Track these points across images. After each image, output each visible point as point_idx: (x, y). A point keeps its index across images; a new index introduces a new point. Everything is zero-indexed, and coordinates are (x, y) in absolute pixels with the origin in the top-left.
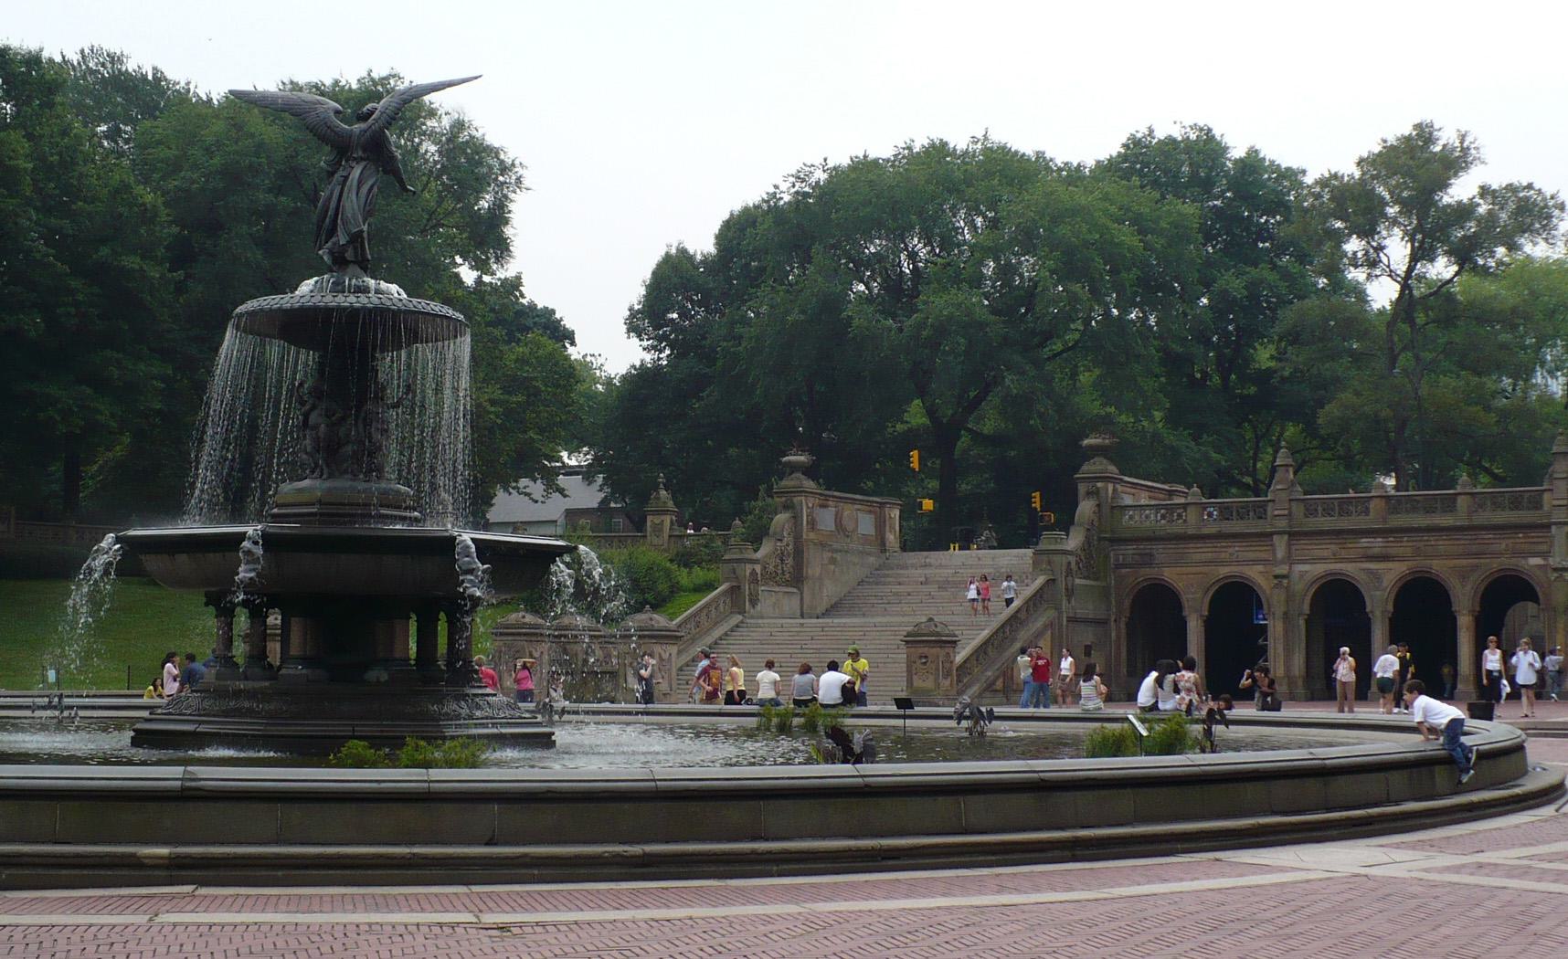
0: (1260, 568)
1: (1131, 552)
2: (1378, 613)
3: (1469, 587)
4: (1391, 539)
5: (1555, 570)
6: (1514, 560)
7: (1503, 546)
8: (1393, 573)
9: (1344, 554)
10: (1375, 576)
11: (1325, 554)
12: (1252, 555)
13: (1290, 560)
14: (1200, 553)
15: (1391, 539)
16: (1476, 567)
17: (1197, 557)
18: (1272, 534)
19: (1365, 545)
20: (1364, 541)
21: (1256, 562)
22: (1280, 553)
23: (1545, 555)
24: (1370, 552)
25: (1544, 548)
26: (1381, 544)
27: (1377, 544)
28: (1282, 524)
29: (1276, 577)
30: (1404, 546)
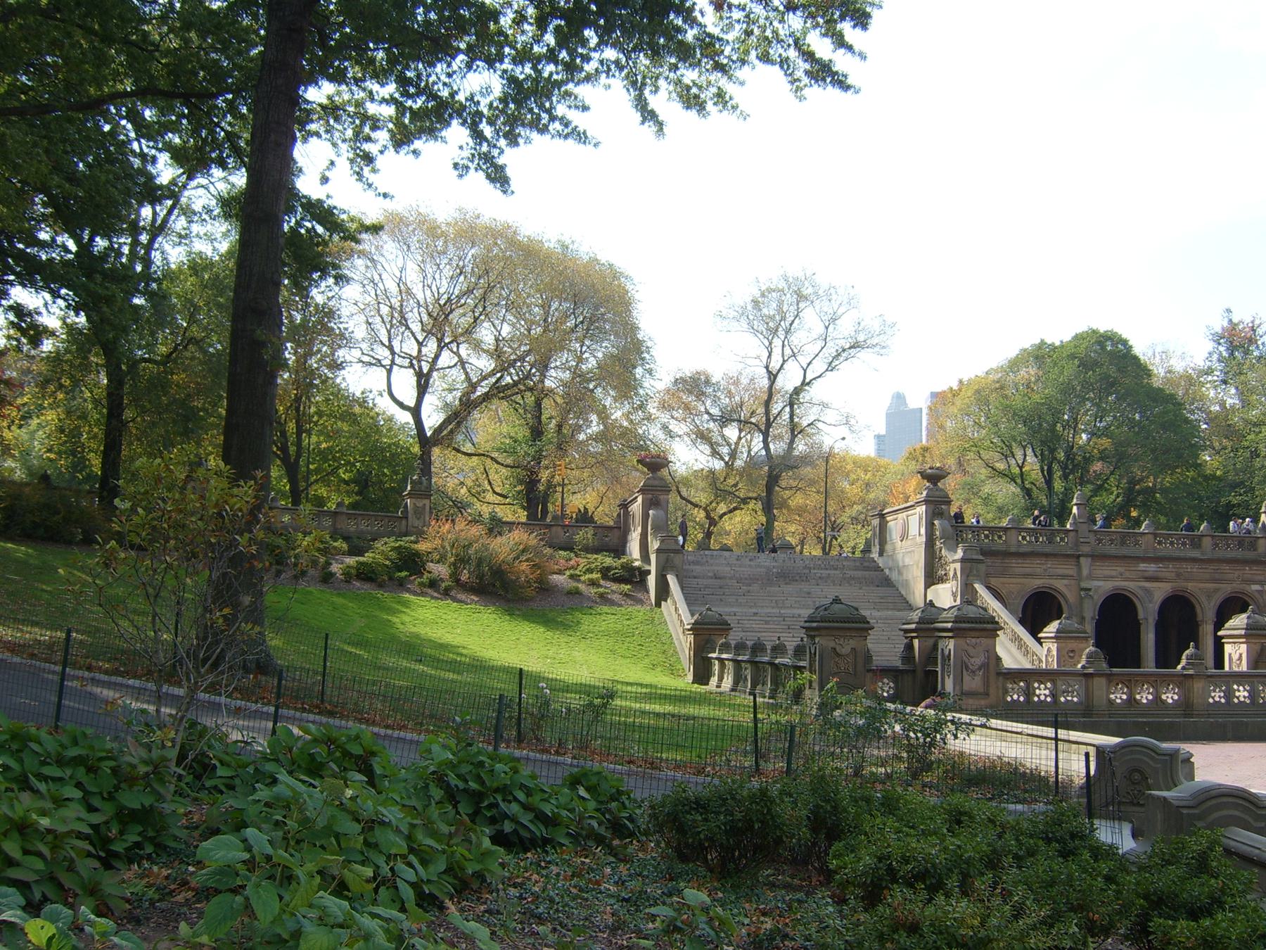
0: (1065, 582)
3: (1212, 604)
6: (1241, 586)
8: (1160, 591)
9: (1127, 574)
10: (1146, 590)
11: (1114, 573)
12: (1060, 572)
13: (1091, 577)
14: (1017, 566)
16: (1216, 590)
17: (1018, 571)
18: (1079, 557)
20: (1142, 566)
21: (1064, 577)
22: (1085, 572)
24: (1146, 574)
27: (1151, 568)
28: (1086, 549)
30: (1168, 570)
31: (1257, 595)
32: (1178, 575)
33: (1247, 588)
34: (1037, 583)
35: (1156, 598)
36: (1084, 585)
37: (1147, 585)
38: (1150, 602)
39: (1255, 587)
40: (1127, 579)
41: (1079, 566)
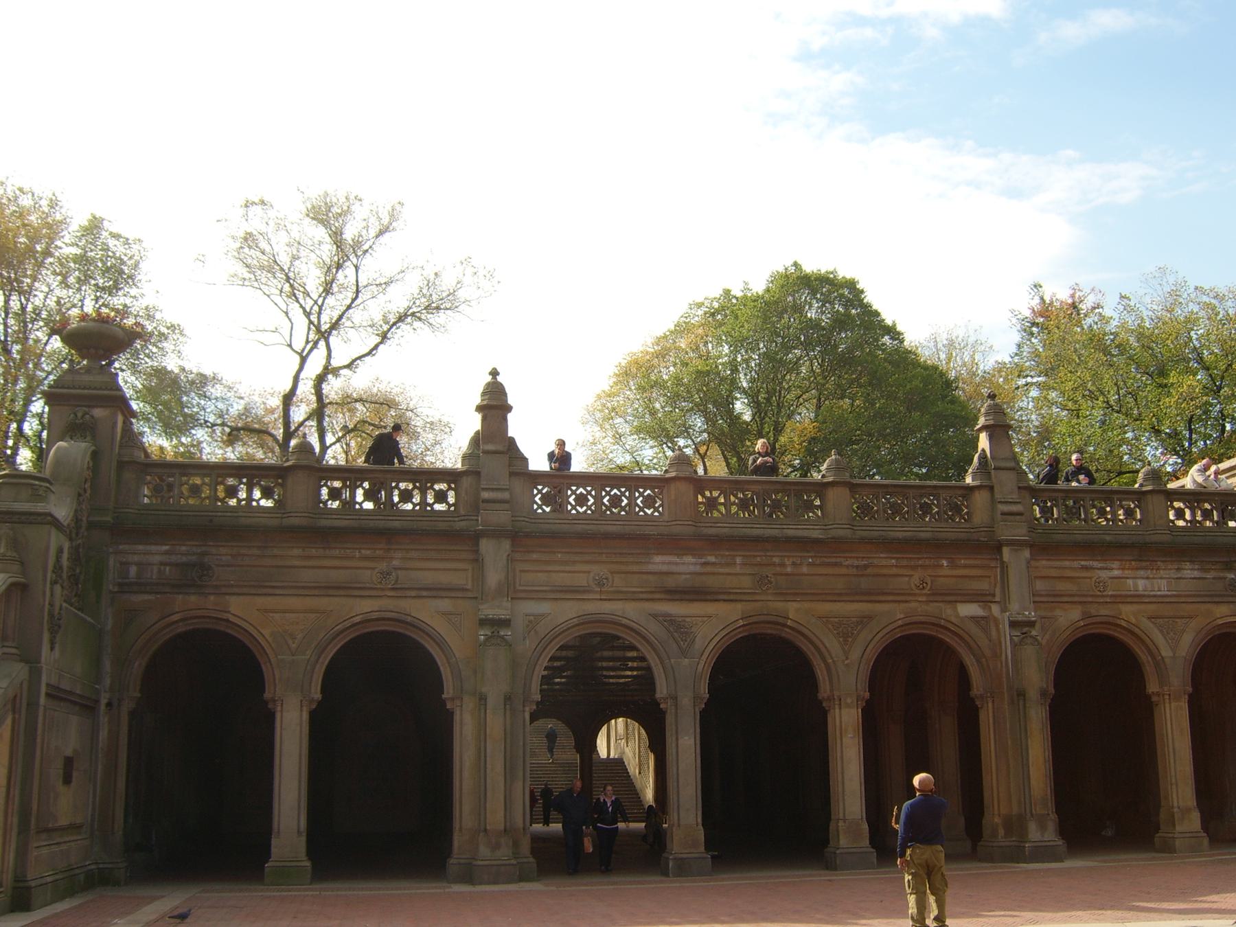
0: (445, 604)
1: (157, 559)
2: (686, 701)
3: (855, 655)
4: (712, 559)
5: (1014, 624)
7: (915, 580)
10: (676, 627)
11: (581, 580)
12: (429, 578)
13: (510, 590)
15: (712, 559)
16: (865, 620)
19: (665, 568)
20: (660, 562)
21: (436, 591)
22: (494, 577)
23: (983, 598)
24: (670, 582)
25: (984, 586)
26: (692, 568)
29: (484, 622)
31: (974, 630)
33: (947, 611)
34: (365, 607)
35: (699, 644)
36: (490, 610)
37: (676, 609)
38: (684, 653)
39: (968, 610)
41: (477, 561)
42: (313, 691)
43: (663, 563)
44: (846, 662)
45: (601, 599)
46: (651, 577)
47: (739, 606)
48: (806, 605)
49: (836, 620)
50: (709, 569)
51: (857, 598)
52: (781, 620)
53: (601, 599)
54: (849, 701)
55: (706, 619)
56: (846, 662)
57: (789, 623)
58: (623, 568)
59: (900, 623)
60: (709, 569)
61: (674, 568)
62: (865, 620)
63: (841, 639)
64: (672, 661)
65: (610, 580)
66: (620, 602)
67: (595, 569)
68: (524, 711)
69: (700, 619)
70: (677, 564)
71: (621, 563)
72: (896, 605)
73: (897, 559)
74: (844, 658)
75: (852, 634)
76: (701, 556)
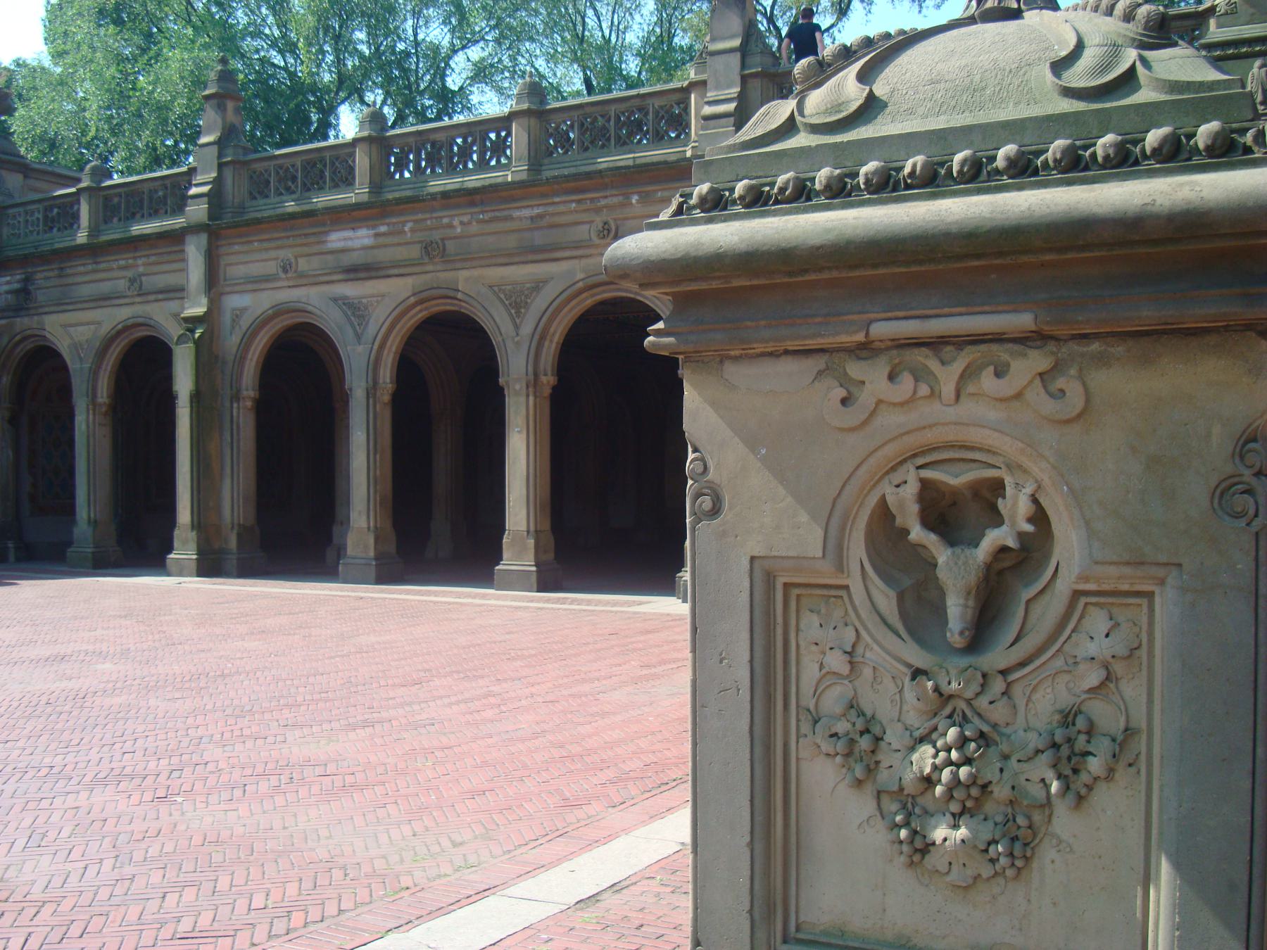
9: (303, 264)
10: (356, 311)
20: (337, 239)
32: (433, 250)
37: (350, 290)
40: (305, 280)
42: (99, 395)
43: (340, 240)
44: (516, 339)
45: (289, 287)
46: (329, 257)
47: (409, 281)
48: (475, 273)
49: (508, 287)
50: (381, 240)
51: (531, 257)
52: (451, 293)
53: (289, 287)
54: (517, 387)
55: (379, 299)
56: (516, 339)
57: (460, 296)
58: (306, 250)
59: (581, 285)
60: (381, 240)
61: (350, 244)
62: (541, 284)
63: (513, 311)
64: (349, 348)
65: (294, 265)
66: (304, 288)
67: (282, 254)
68: (232, 407)
69: (375, 299)
70: (351, 239)
71: (305, 245)
72: (576, 261)
73: (579, 201)
74: (515, 334)
75: (526, 303)
76: (374, 227)
